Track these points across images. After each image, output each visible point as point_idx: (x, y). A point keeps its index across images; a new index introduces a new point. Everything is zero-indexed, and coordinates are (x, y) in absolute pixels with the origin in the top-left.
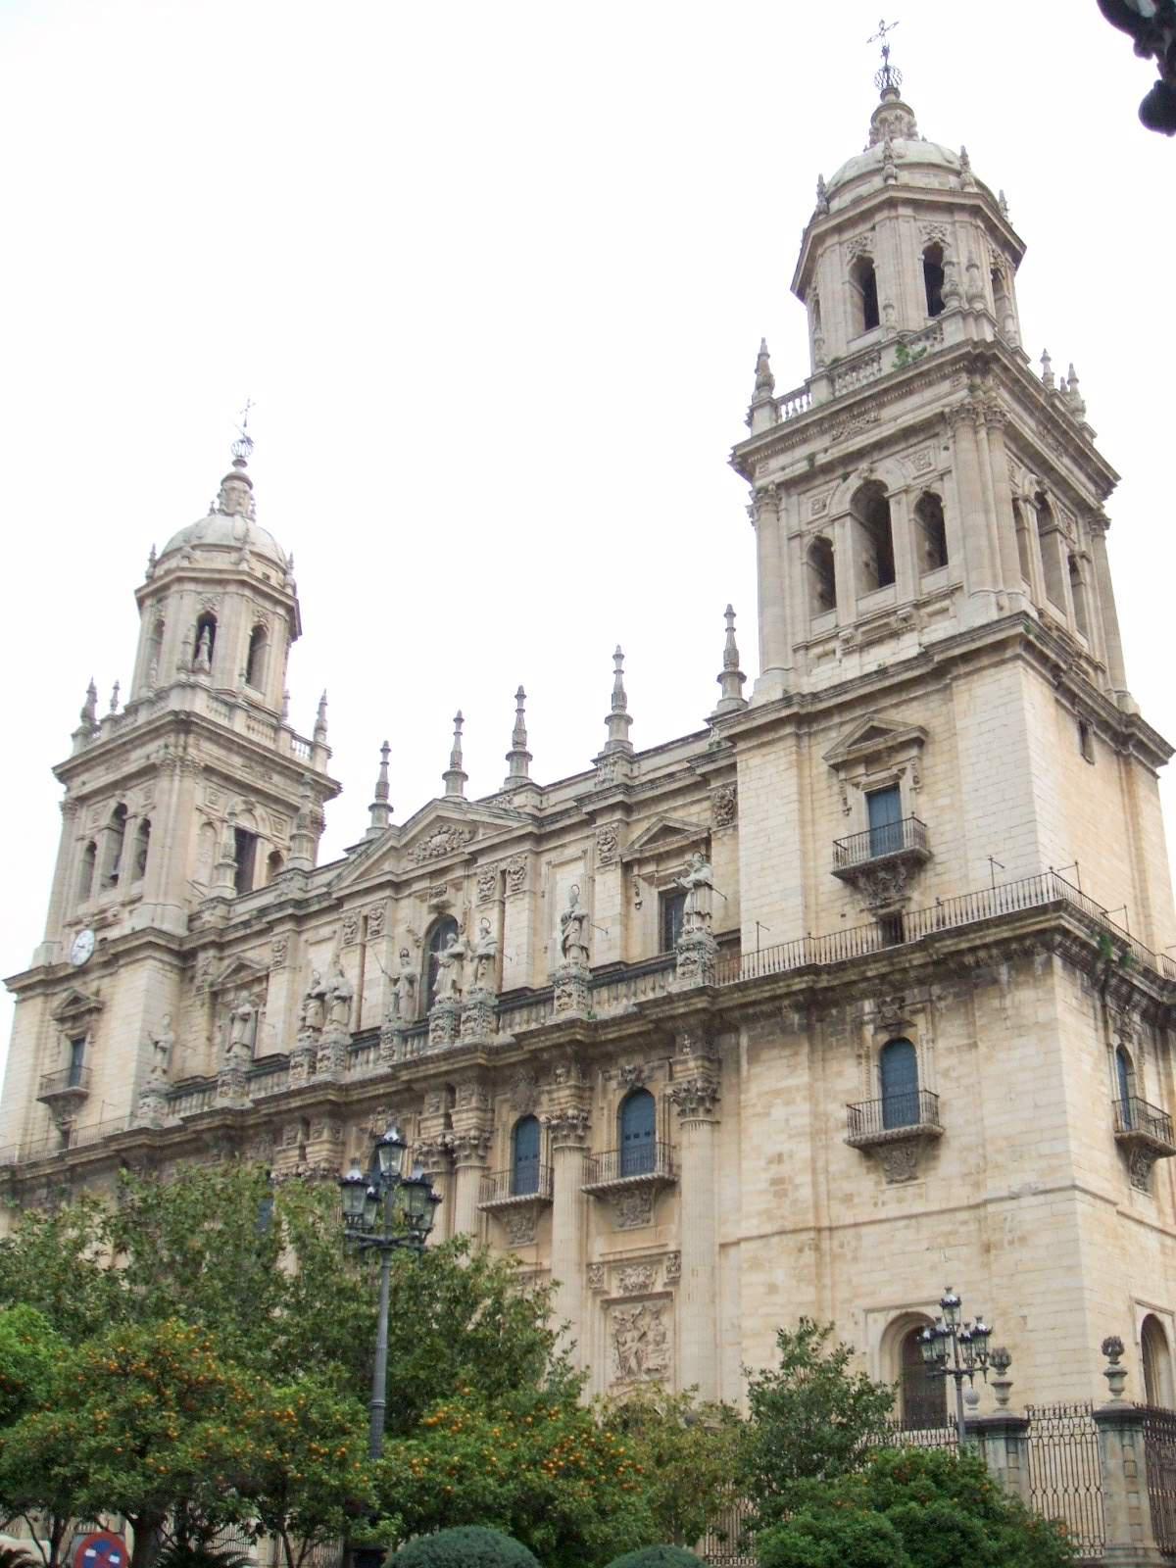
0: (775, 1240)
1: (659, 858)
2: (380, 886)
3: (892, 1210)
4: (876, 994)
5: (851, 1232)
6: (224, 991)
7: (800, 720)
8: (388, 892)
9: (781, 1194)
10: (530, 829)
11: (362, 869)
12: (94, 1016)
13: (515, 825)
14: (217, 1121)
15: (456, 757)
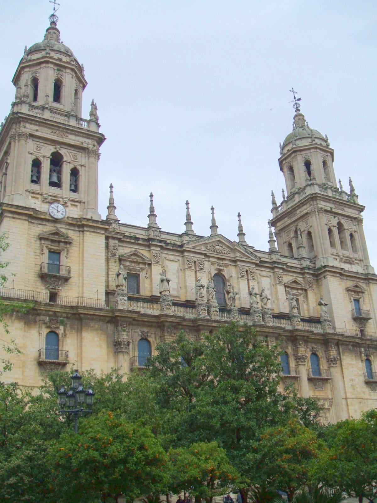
0: (354, 399)
1: (292, 288)
2: (202, 254)
3: (372, 397)
4: (364, 347)
5: (366, 400)
6: (125, 260)
7: (341, 274)
8: (203, 257)
9: (354, 389)
10: (258, 262)
11: (196, 245)
12: (68, 246)
13: (254, 259)
14: (178, 320)
15: (213, 221)
